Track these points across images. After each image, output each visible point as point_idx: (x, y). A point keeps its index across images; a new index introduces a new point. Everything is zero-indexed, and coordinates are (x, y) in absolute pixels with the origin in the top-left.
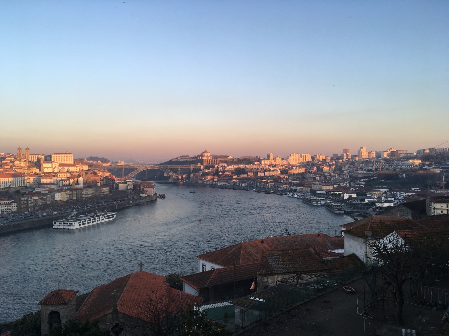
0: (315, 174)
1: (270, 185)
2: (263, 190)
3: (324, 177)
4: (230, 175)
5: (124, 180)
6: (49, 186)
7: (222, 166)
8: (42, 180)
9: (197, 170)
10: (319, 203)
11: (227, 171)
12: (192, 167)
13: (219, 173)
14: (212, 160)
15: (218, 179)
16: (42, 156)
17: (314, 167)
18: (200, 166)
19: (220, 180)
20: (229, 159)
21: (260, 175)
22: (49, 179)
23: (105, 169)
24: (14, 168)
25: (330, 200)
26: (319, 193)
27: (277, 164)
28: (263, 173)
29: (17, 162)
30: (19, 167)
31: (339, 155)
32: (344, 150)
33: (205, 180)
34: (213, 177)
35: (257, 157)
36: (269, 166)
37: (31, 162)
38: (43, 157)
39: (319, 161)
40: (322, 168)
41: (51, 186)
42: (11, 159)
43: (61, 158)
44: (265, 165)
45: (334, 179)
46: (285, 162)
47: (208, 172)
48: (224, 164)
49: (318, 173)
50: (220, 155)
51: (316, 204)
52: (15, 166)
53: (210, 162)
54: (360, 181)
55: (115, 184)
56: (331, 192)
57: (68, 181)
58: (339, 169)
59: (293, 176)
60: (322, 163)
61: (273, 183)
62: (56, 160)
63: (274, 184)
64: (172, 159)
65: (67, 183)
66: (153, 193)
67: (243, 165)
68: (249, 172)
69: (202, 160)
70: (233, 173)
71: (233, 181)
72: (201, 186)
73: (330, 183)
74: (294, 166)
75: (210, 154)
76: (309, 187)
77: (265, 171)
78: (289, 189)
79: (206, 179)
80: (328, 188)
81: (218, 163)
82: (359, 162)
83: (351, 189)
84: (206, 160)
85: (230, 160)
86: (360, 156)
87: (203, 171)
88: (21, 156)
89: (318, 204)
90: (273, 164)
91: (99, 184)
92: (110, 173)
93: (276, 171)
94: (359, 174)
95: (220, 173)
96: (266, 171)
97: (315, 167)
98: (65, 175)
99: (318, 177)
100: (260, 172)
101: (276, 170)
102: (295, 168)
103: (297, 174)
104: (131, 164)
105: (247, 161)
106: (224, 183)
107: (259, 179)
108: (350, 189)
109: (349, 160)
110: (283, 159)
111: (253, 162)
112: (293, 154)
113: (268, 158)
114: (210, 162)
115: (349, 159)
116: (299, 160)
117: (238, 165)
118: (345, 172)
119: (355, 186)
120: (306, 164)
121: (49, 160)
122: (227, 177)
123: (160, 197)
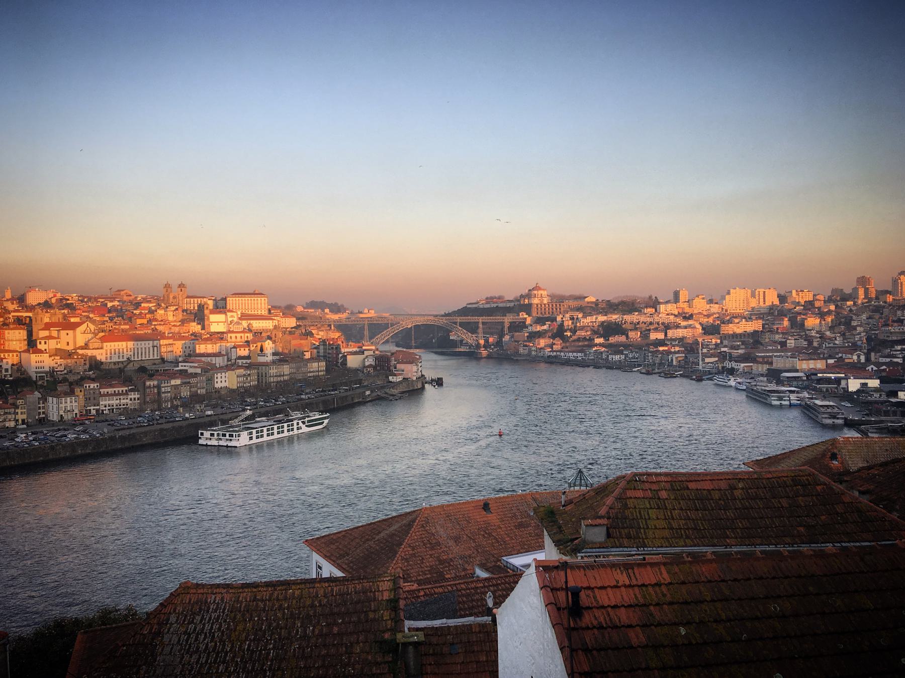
0: (786, 334)
1: (675, 359)
2: (658, 369)
3: (805, 340)
4: (588, 338)
5: (358, 347)
6: (209, 359)
7: (572, 318)
8: (197, 346)
9: (518, 326)
10: (785, 400)
11: (582, 328)
12: (508, 319)
13: (565, 334)
14: (551, 306)
15: (563, 345)
16: (209, 299)
17: (783, 319)
18: (526, 319)
19: (567, 348)
20: (588, 303)
21: (653, 336)
22: (211, 345)
23: (331, 325)
24: (153, 323)
25: (811, 393)
26: (788, 377)
27: (696, 312)
28: (661, 331)
29: (161, 312)
30: (165, 322)
31: (848, 291)
32: (858, 278)
33: (534, 348)
34: (552, 340)
35: (650, 297)
36: (676, 316)
37: (188, 312)
38: (211, 303)
39: (798, 304)
40: (803, 320)
41: (214, 358)
42: (151, 305)
43: (245, 303)
44: (668, 314)
45: (831, 345)
46: (715, 308)
47: (540, 330)
48: (577, 313)
49: (793, 332)
50: (567, 294)
51: (778, 403)
52: (156, 320)
53: (547, 309)
54: (893, 349)
55: (340, 355)
56: (819, 375)
57: (247, 349)
58: (844, 323)
59: (733, 338)
60: (804, 309)
61: (684, 355)
62: (236, 307)
63: (686, 357)
64: (467, 304)
65: (244, 352)
66: (415, 374)
67: (618, 316)
68: (631, 330)
69: (530, 305)
70: (596, 332)
71: (594, 349)
72: (526, 360)
73: (819, 354)
74: (736, 317)
75: (545, 292)
76: (766, 363)
77: (667, 327)
78: (720, 368)
79: (537, 344)
80: (812, 366)
81: (564, 311)
82: (894, 306)
83: (869, 368)
84: (537, 306)
85: (590, 305)
86: (898, 292)
87: (530, 328)
88: (171, 300)
89: (784, 403)
90: (687, 313)
91: (308, 355)
92: (339, 332)
93: (692, 328)
94: (891, 333)
95: (566, 331)
96: (668, 329)
97: (787, 319)
98: (241, 337)
99: (793, 341)
100: (656, 330)
101: (691, 325)
102: (736, 321)
103: (740, 335)
104: (387, 315)
105: (629, 306)
106: (575, 354)
107: (651, 344)
108: (867, 369)
109: (870, 301)
110: (711, 301)
111: (642, 308)
112: (735, 289)
113: (676, 298)
114: (547, 309)
115: (870, 300)
116: (748, 303)
117: (606, 315)
118: (858, 328)
119: (880, 361)
120: (766, 311)
121: (223, 308)
122: (583, 341)
123: (432, 382)
